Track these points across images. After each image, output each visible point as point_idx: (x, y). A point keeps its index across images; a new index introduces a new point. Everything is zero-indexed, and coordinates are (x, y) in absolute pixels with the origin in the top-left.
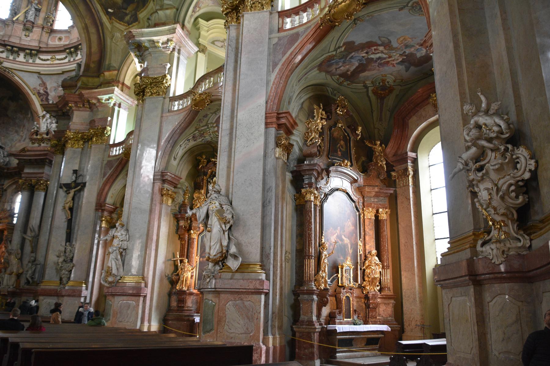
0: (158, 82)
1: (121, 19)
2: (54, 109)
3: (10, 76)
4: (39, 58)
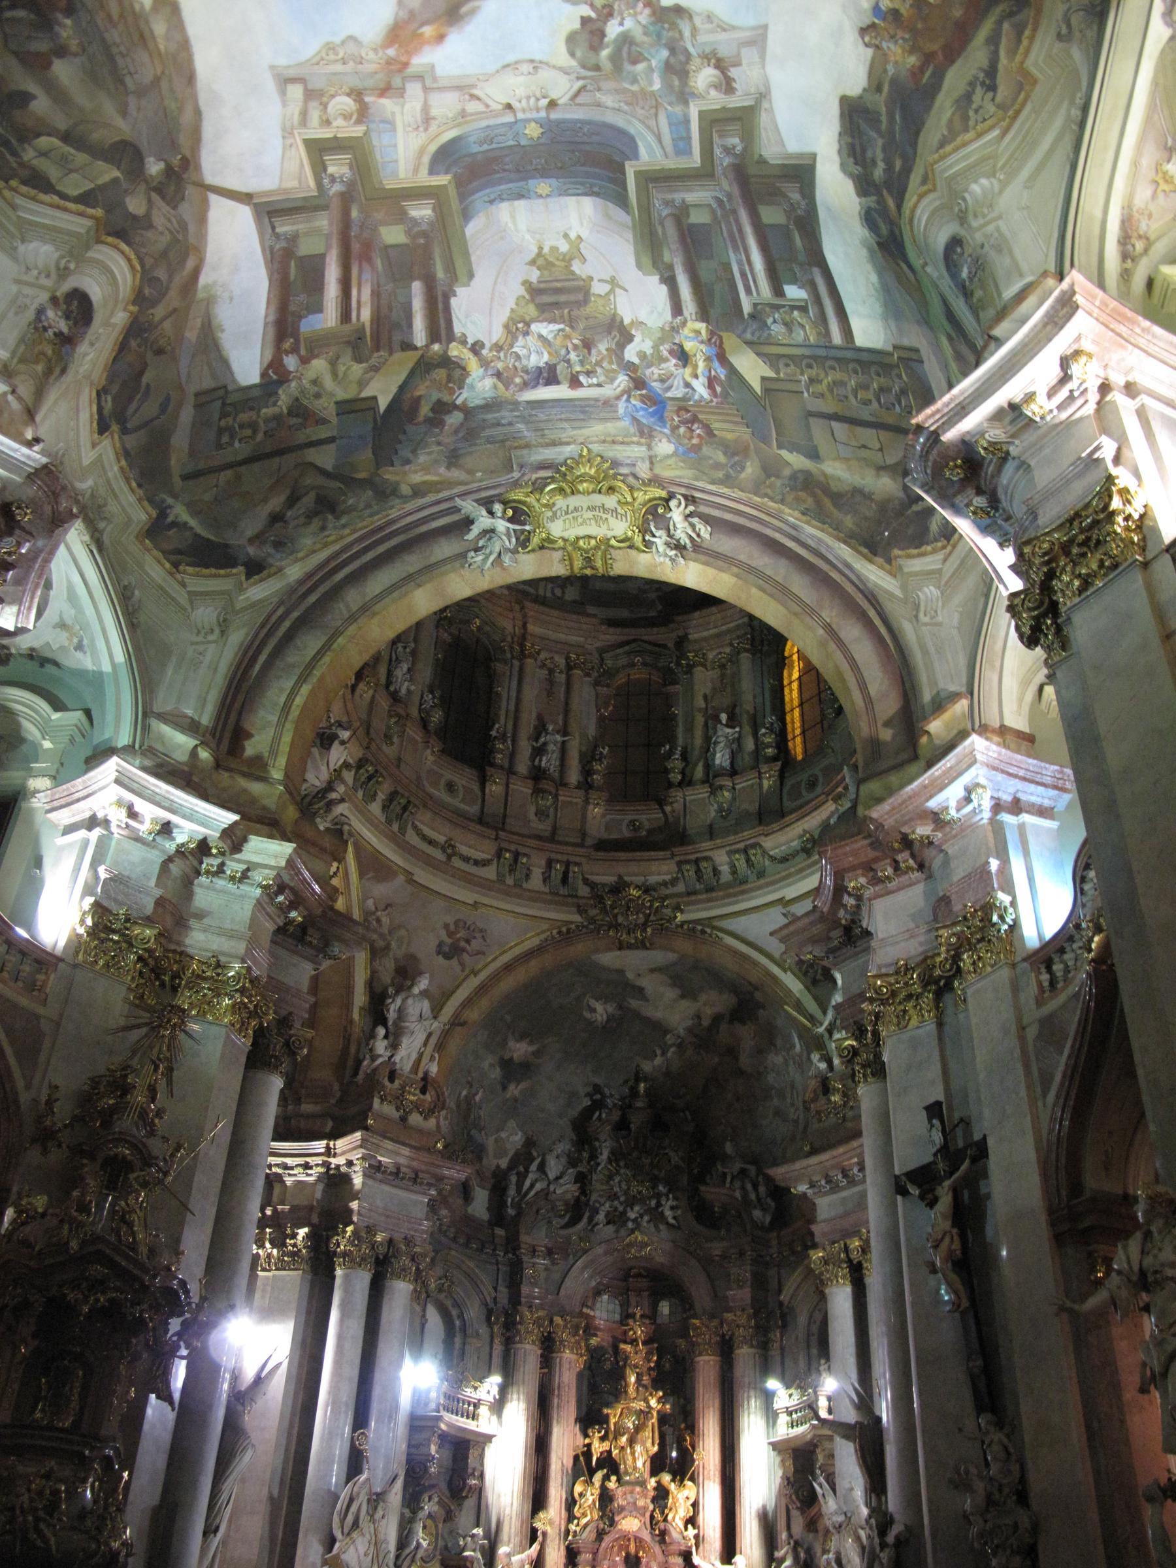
0: (1096, 523)
2: (815, 930)
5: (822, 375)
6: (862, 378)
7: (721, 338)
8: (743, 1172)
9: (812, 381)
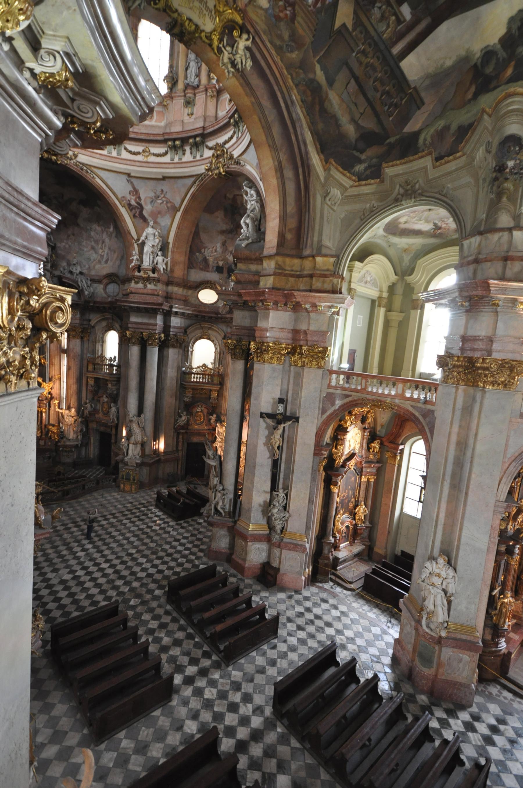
1: (347, 165)
3: (89, 176)
4: (126, 149)
5: (370, 55)
8: (81, 273)
9: (364, 53)
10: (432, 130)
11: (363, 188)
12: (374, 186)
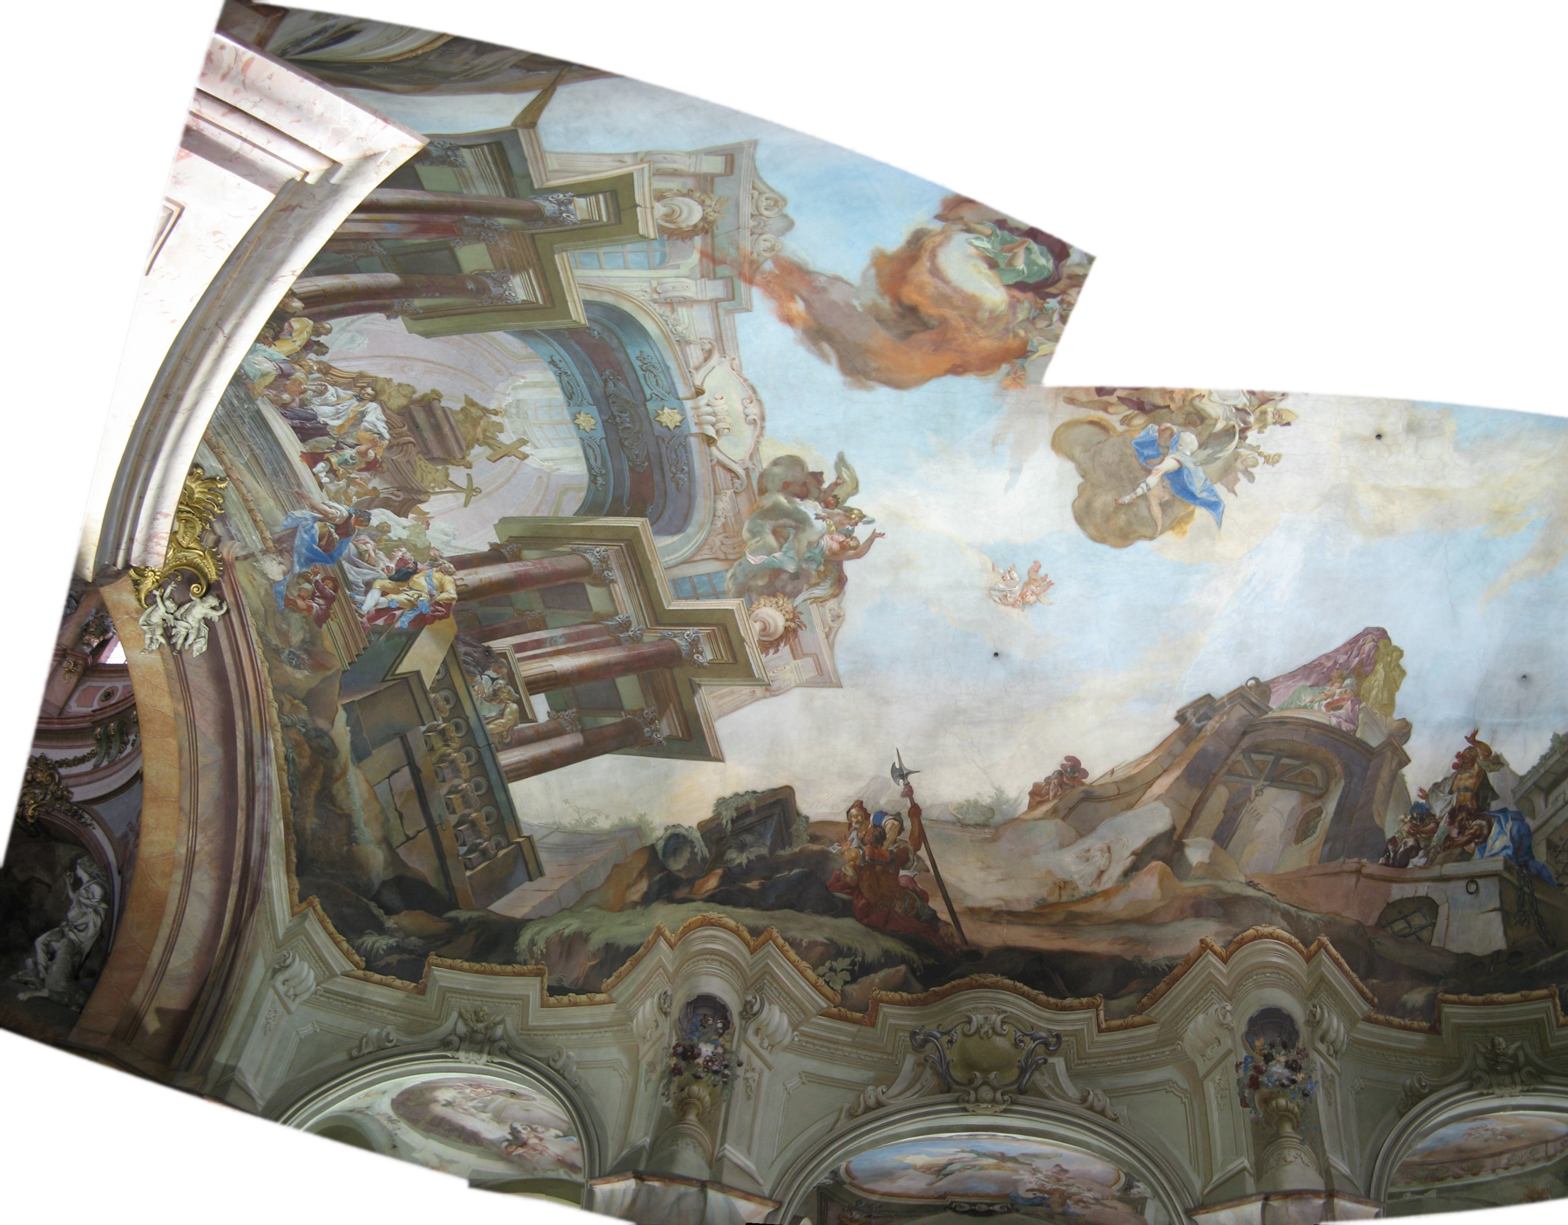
1: (349, 925)
5: (454, 745)
6: (473, 795)
7: (446, 616)
9: (442, 733)
10: (551, 931)
11: (371, 987)
12: (400, 995)
